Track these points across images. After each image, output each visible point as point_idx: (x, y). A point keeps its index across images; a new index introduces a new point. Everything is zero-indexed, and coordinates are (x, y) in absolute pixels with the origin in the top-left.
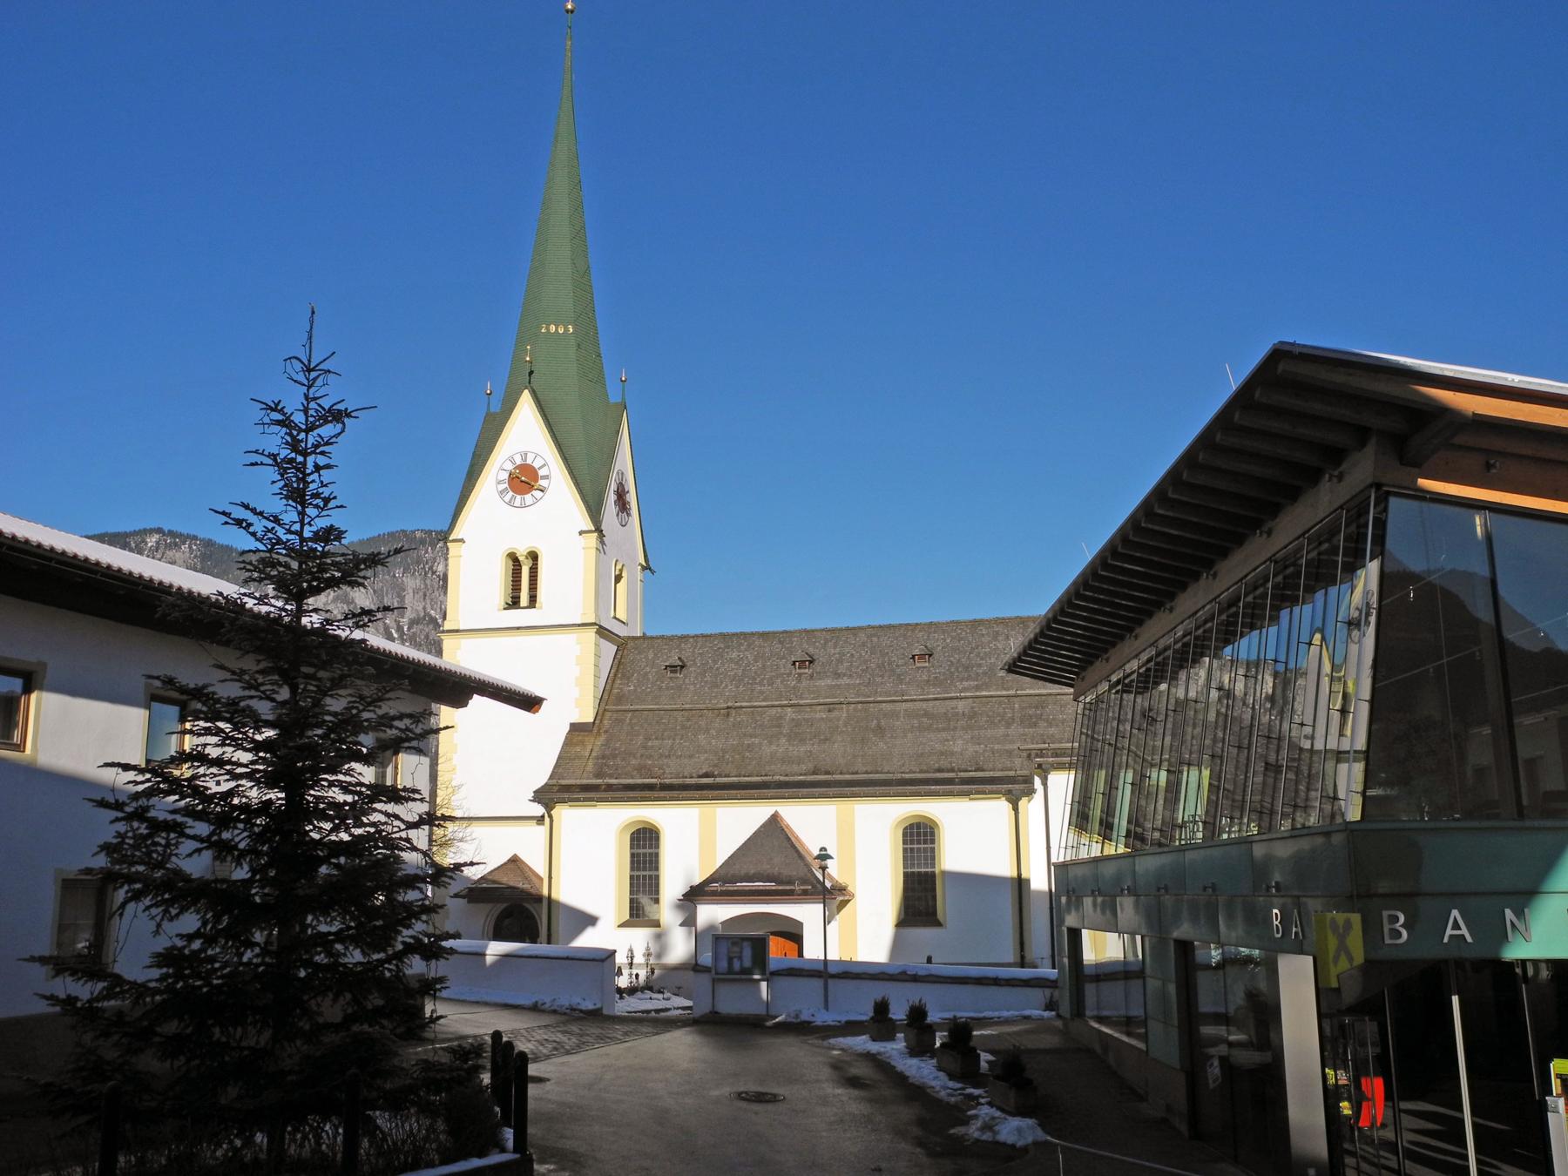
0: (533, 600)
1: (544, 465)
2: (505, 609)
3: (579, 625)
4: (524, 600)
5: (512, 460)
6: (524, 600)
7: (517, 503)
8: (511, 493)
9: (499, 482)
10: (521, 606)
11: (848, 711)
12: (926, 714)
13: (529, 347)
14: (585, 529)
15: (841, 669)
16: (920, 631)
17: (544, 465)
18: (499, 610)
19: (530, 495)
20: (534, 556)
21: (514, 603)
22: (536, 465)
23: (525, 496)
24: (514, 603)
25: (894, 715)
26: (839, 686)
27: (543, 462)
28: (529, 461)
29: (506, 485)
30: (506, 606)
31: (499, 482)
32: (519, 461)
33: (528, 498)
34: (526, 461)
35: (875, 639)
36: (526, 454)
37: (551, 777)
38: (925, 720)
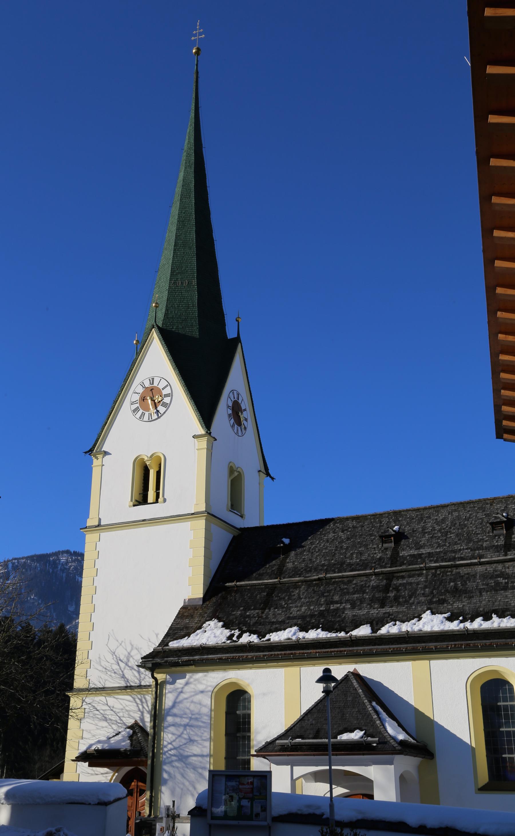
2: (134, 506)
3: (192, 514)
7: (146, 418)
8: (141, 411)
10: (148, 502)
11: (427, 576)
12: (502, 575)
14: (200, 433)
15: (423, 541)
16: (498, 503)
18: (130, 506)
21: (143, 500)
22: (161, 387)
24: (143, 500)
25: (472, 577)
26: (420, 556)
29: (138, 405)
30: (137, 503)
34: (153, 384)
35: (456, 514)
36: (153, 379)
37: (160, 645)
38: (500, 580)
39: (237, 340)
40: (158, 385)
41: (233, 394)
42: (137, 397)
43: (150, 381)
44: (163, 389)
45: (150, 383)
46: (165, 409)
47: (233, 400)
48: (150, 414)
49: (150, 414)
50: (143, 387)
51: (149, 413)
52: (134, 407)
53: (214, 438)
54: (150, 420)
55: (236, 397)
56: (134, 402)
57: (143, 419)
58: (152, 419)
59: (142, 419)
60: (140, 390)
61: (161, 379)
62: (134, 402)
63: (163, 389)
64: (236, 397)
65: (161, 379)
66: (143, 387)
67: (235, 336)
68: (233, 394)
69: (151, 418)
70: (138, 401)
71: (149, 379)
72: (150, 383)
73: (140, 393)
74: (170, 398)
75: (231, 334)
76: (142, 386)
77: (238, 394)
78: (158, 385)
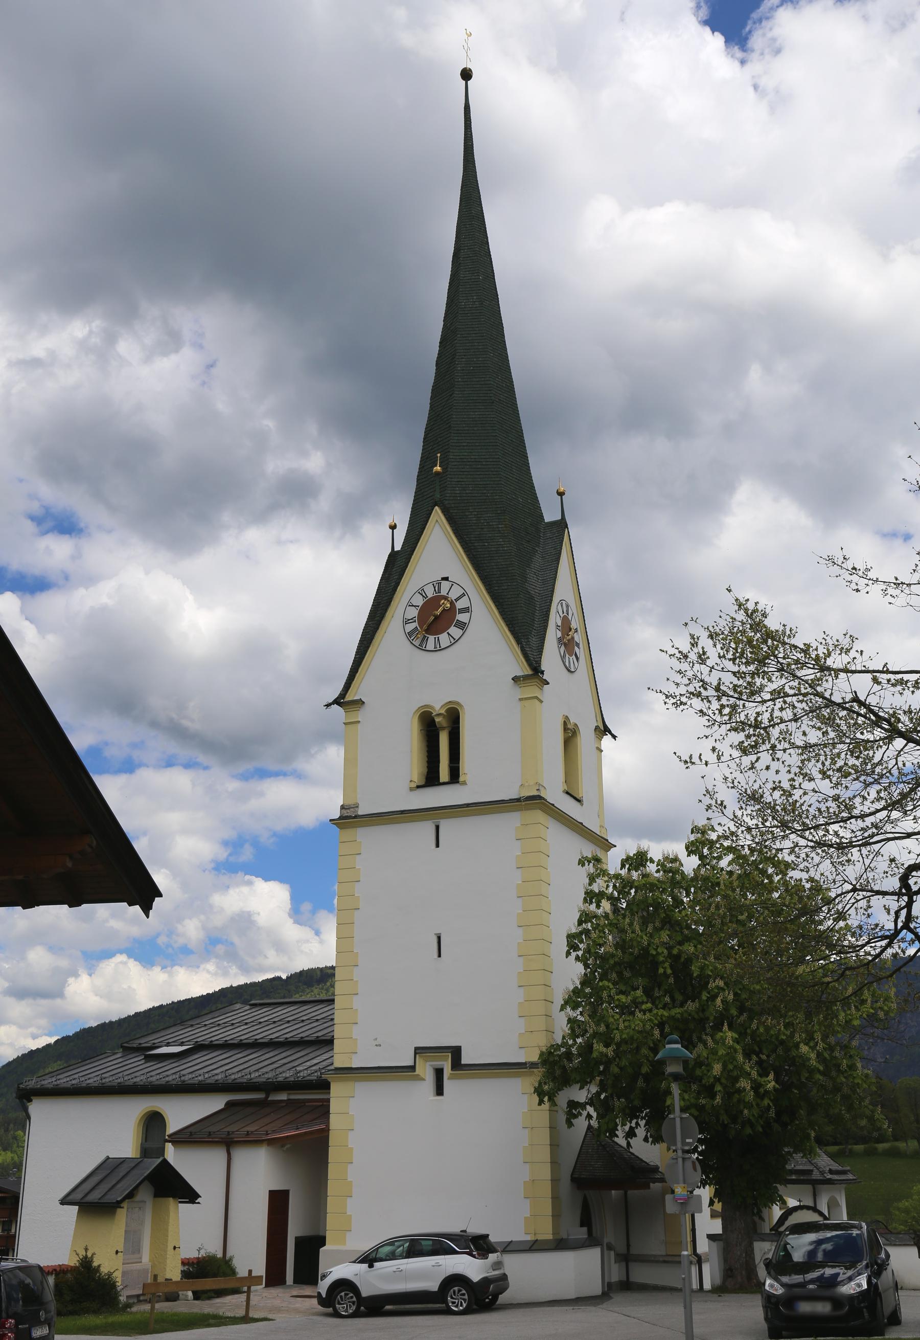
0: (455, 776)
1: (463, 595)
4: (444, 775)
5: (421, 592)
6: (444, 775)
7: (430, 645)
9: (407, 622)
10: (442, 780)
13: (439, 455)
14: (520, 673)
17: (463, 595)
18: (411, 789)
19: (445, 634)
20: (454, 717)
21: (431, 779)
23: (440, 636)
24: (431, 779)
27: (461, 592)
28: (444, 592)
31: (407, 622)
32: (430, 593)
33: (444, 638)
39: (561, 526)
40: (448, 594)
41: (562, 606)
42: (413, 613)
43: (435, 588)
44: (457, 600)
45: (435, 590)
46: (461, 632)
47: (562, 616)
48: (437, 639)
49: (437, 639)
50: (423, 596)
51: (435, 638)
52: (410, 627)
53: (545, 680)
54: (438, 649)
55: (565, 611)
56: (409, 620)
57: (425, 647)
58: (440, 647)
59: (424, 646)
60: (419, 601)
61: (452, 585)
62: (409, 620)
63: (457, 600)
64: (565, 611)
65: (452, 585)
66: (423, 596)
67: (558, 517)
68: (562, 606)
69: (438, 646)
70: (416, 619)
71: (433, 584)
72: (435, 590)
73: (418, 606)
74: (468, 615)
75: (550, 515)
76: (422, 595)
77: (567, 606)
78: (448, 594)
